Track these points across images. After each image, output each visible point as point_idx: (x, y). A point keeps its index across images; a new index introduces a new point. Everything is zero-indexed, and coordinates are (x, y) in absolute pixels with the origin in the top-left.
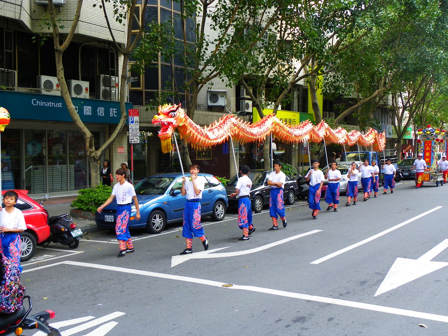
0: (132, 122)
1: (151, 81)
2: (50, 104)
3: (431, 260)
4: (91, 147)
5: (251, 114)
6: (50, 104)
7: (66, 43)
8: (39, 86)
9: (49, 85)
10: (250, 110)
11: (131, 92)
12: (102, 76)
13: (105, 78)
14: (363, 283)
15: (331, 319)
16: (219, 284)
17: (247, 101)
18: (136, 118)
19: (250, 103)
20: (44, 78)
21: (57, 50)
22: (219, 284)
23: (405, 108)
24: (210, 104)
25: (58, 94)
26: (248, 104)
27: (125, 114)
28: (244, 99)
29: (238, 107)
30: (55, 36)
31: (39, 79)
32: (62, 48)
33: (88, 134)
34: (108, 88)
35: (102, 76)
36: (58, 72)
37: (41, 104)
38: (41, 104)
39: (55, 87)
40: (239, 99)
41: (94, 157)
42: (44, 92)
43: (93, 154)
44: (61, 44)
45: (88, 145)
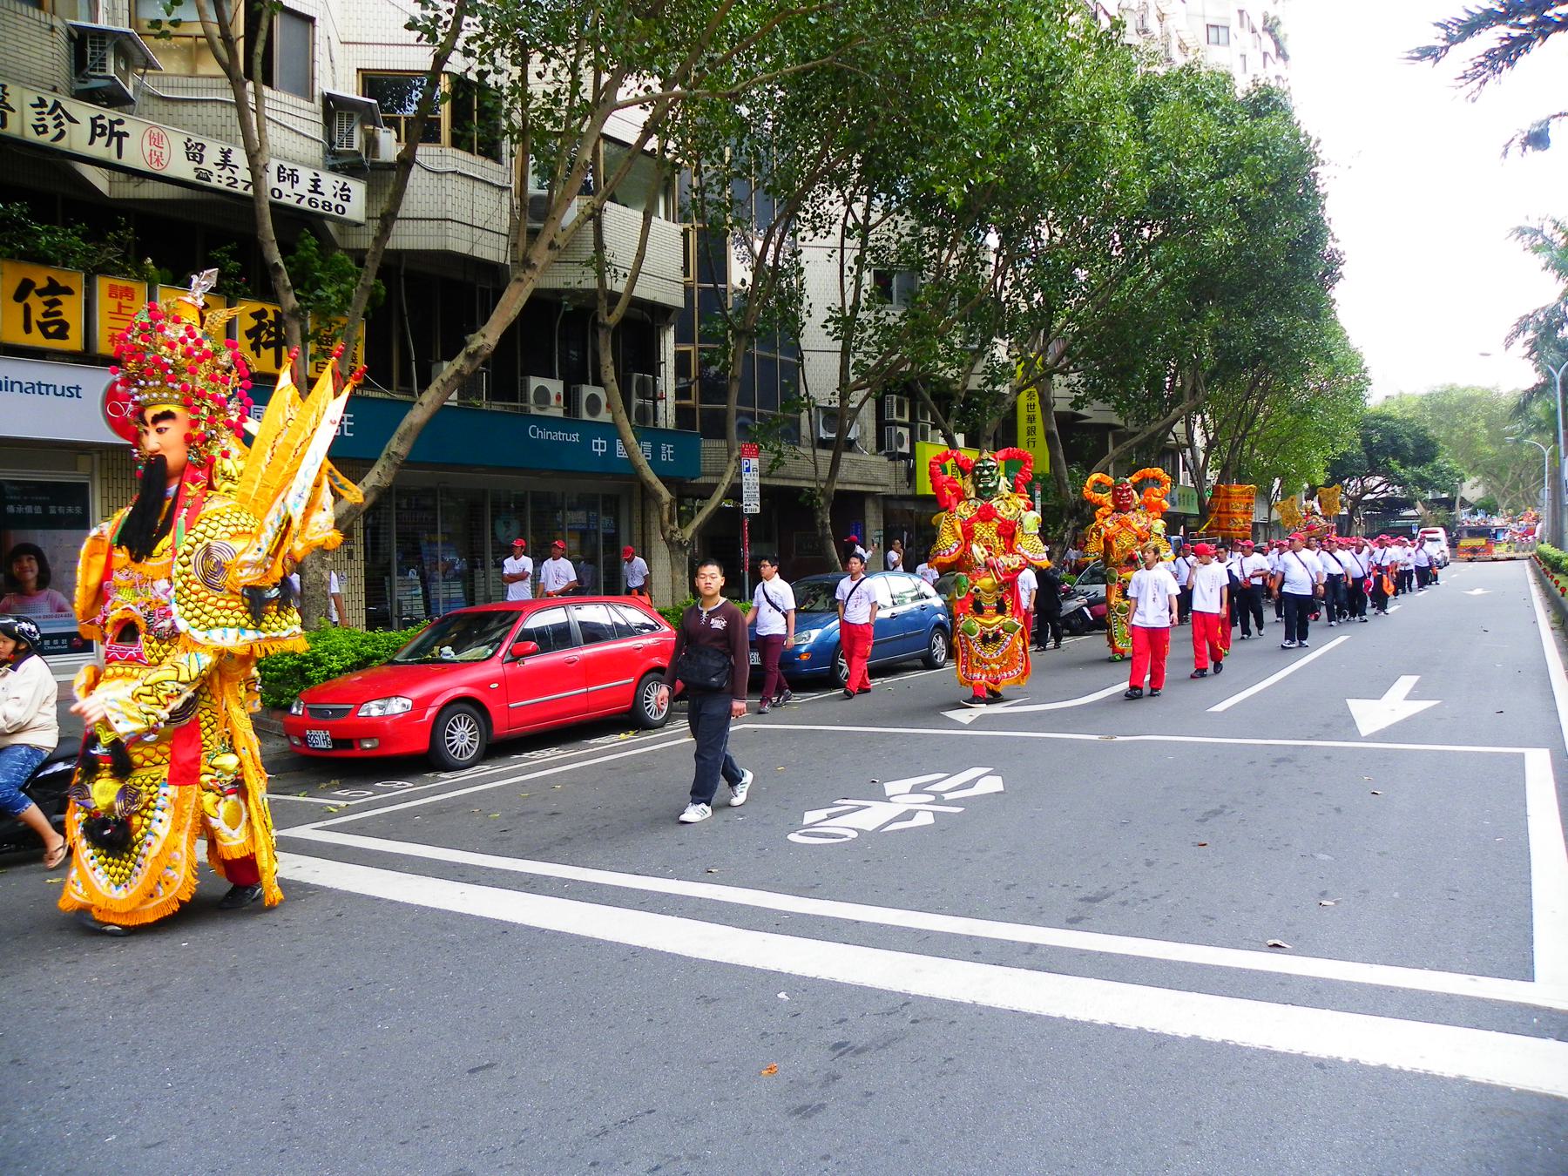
0: (748, 470)
1: (713, 389)
2: (559, 436)
3: (1407, 698)
4: (671, 521)
5: (912, 455)
6: (559, 436)
7: (620, 310)
8: (525, 399)
9: (542, 393)
10: (906, 449)
11: (678, 409)
12: (636, 376)
13: (642, 382)
14: (1327, 726)
15: (1328, 758)
16: (1095, 737)
17: (900, 430)
18: (754, 462)
19: (906, 432)
20: (535, 382)
21: (604, 326)
22: (1095, 737)
23: (1210, 445)
24: (822, 435)
25: (559, 413)
26: (900, 436)
27: (737, 453)
28: (894, 423)
29: (880, 445)
30: (601, 296)
31: (526, 386)
32: (612, 320)
33: (666, 495)
34: (649, 403)
35: (636, 376)
36: (603, 369)
37: (544, 435)
38: (544, 435)
39: (553, 401)
40: (882, 424)
41: (679, 541)
42: (534, 411)
43: (677, 536)
44: (609, 314)
45: (666, 516)
